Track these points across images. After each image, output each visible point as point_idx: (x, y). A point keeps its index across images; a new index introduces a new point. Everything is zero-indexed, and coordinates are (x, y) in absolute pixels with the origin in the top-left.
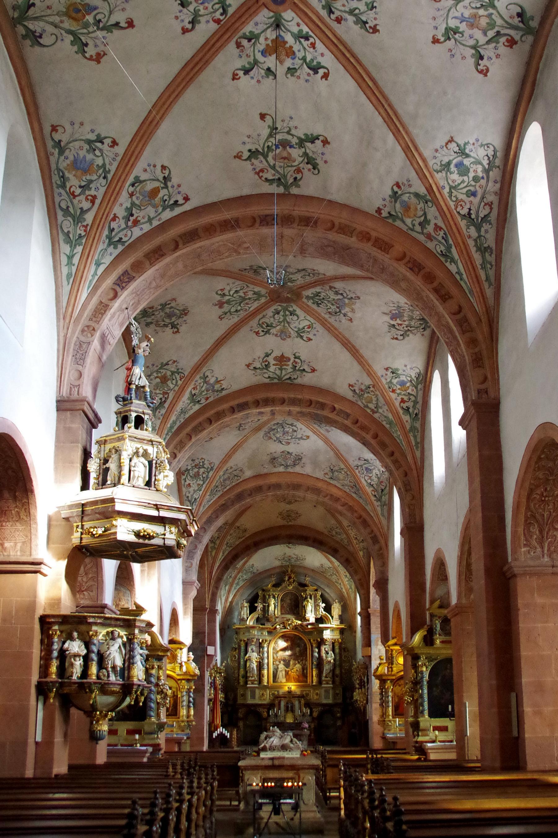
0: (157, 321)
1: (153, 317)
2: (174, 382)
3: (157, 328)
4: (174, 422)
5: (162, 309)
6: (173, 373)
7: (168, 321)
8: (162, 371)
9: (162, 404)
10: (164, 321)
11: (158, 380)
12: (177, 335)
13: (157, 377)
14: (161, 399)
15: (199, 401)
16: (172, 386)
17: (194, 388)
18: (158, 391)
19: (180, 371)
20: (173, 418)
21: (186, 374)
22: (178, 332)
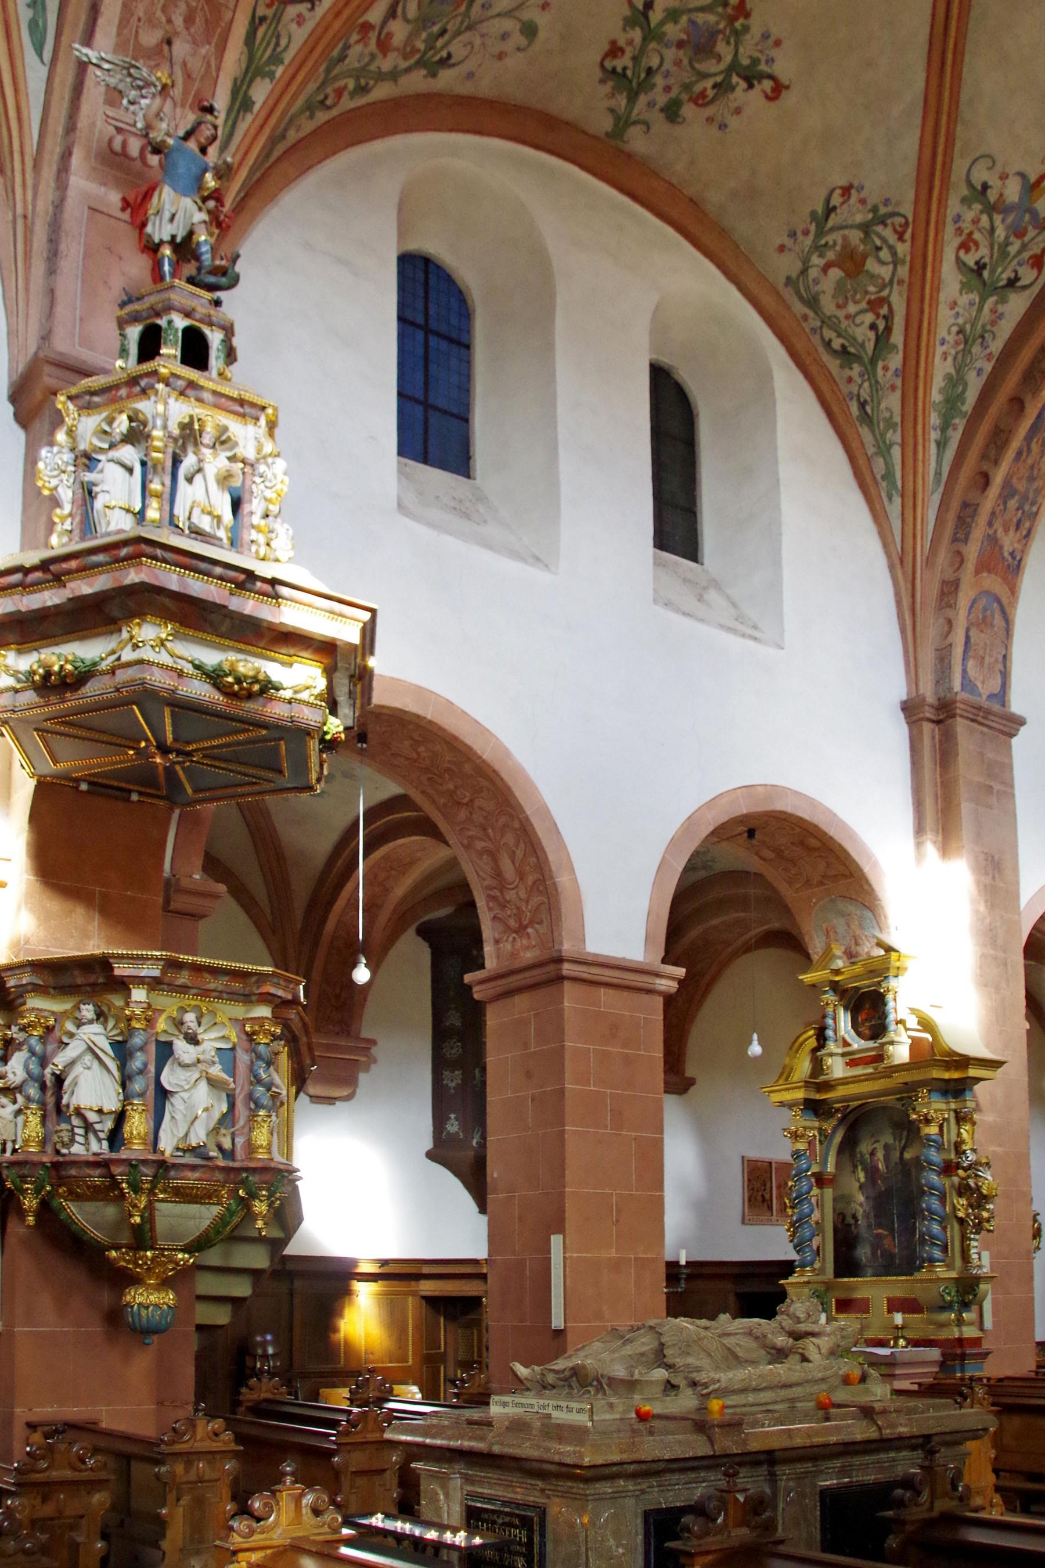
0: (687, 87)
1: (659, 80)
2: (885, 254)
3: (709, 111)
4: (956, 382)
5: (651, 35)
6: (866, 228)
7: (711, 66)
8: (830, 239)
9: (882, 339)
10: (705, 76)
11: (835, 273)
12: (788, 99)
13: (825, 269)
14: (873, 327)
15: (1012, 283)
16: (885, 272)
17: (965, 246)
18: (852, 309)
19: (883, 210)
20: (941, 369)
21: (908, 210)
22: (778, 89)
